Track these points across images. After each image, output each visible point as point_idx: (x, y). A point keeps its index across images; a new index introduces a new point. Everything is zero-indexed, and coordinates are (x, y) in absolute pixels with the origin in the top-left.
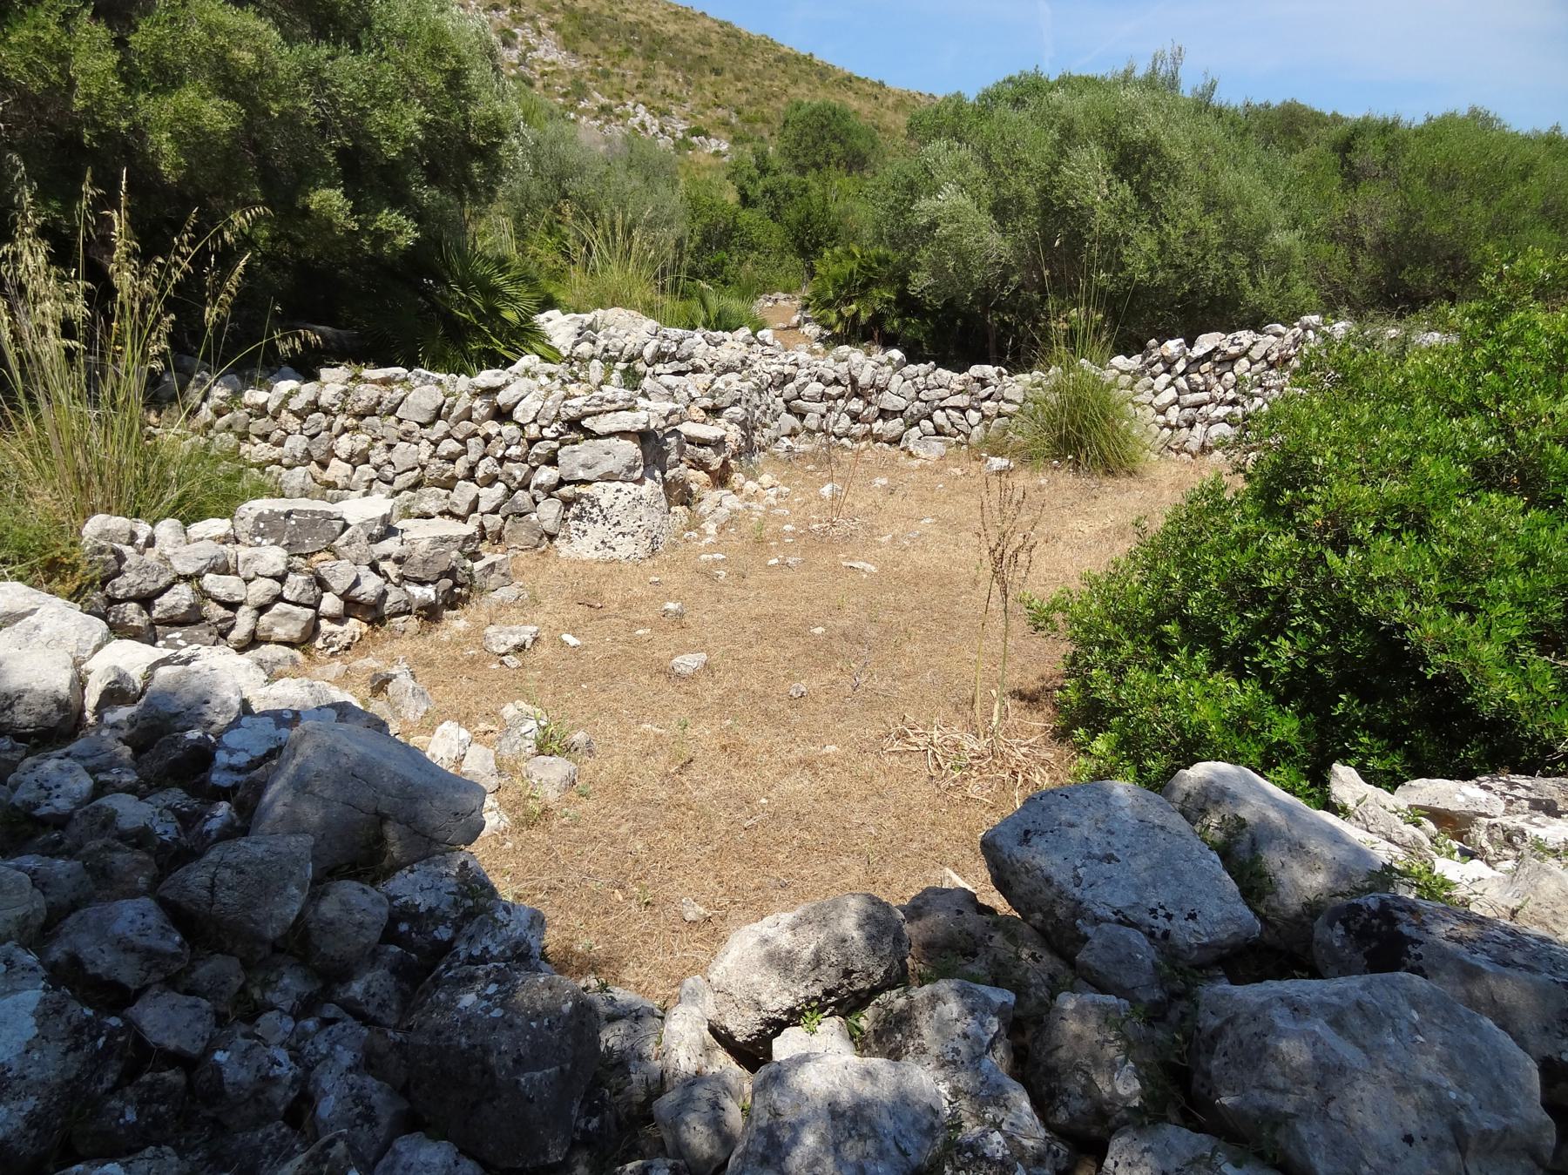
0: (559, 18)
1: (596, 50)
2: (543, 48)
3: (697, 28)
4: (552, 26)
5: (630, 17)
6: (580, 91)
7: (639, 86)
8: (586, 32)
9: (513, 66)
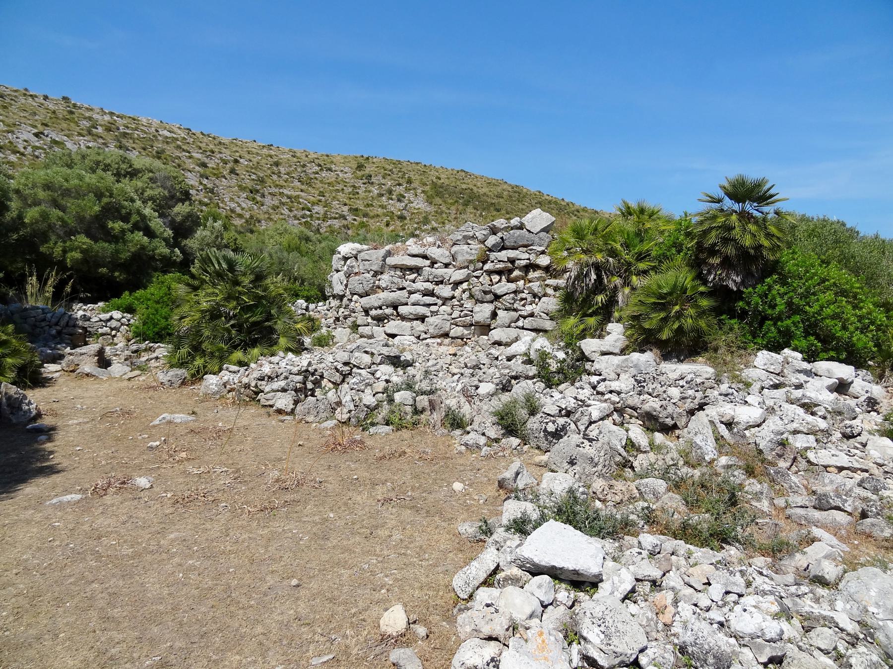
0: (427, 188)
1: (441, 202)
3: (499, 189)
4: (423, 192)
5: (464, 186)
6: (426, 221)
8: (438, 194)
9: (399, 210)
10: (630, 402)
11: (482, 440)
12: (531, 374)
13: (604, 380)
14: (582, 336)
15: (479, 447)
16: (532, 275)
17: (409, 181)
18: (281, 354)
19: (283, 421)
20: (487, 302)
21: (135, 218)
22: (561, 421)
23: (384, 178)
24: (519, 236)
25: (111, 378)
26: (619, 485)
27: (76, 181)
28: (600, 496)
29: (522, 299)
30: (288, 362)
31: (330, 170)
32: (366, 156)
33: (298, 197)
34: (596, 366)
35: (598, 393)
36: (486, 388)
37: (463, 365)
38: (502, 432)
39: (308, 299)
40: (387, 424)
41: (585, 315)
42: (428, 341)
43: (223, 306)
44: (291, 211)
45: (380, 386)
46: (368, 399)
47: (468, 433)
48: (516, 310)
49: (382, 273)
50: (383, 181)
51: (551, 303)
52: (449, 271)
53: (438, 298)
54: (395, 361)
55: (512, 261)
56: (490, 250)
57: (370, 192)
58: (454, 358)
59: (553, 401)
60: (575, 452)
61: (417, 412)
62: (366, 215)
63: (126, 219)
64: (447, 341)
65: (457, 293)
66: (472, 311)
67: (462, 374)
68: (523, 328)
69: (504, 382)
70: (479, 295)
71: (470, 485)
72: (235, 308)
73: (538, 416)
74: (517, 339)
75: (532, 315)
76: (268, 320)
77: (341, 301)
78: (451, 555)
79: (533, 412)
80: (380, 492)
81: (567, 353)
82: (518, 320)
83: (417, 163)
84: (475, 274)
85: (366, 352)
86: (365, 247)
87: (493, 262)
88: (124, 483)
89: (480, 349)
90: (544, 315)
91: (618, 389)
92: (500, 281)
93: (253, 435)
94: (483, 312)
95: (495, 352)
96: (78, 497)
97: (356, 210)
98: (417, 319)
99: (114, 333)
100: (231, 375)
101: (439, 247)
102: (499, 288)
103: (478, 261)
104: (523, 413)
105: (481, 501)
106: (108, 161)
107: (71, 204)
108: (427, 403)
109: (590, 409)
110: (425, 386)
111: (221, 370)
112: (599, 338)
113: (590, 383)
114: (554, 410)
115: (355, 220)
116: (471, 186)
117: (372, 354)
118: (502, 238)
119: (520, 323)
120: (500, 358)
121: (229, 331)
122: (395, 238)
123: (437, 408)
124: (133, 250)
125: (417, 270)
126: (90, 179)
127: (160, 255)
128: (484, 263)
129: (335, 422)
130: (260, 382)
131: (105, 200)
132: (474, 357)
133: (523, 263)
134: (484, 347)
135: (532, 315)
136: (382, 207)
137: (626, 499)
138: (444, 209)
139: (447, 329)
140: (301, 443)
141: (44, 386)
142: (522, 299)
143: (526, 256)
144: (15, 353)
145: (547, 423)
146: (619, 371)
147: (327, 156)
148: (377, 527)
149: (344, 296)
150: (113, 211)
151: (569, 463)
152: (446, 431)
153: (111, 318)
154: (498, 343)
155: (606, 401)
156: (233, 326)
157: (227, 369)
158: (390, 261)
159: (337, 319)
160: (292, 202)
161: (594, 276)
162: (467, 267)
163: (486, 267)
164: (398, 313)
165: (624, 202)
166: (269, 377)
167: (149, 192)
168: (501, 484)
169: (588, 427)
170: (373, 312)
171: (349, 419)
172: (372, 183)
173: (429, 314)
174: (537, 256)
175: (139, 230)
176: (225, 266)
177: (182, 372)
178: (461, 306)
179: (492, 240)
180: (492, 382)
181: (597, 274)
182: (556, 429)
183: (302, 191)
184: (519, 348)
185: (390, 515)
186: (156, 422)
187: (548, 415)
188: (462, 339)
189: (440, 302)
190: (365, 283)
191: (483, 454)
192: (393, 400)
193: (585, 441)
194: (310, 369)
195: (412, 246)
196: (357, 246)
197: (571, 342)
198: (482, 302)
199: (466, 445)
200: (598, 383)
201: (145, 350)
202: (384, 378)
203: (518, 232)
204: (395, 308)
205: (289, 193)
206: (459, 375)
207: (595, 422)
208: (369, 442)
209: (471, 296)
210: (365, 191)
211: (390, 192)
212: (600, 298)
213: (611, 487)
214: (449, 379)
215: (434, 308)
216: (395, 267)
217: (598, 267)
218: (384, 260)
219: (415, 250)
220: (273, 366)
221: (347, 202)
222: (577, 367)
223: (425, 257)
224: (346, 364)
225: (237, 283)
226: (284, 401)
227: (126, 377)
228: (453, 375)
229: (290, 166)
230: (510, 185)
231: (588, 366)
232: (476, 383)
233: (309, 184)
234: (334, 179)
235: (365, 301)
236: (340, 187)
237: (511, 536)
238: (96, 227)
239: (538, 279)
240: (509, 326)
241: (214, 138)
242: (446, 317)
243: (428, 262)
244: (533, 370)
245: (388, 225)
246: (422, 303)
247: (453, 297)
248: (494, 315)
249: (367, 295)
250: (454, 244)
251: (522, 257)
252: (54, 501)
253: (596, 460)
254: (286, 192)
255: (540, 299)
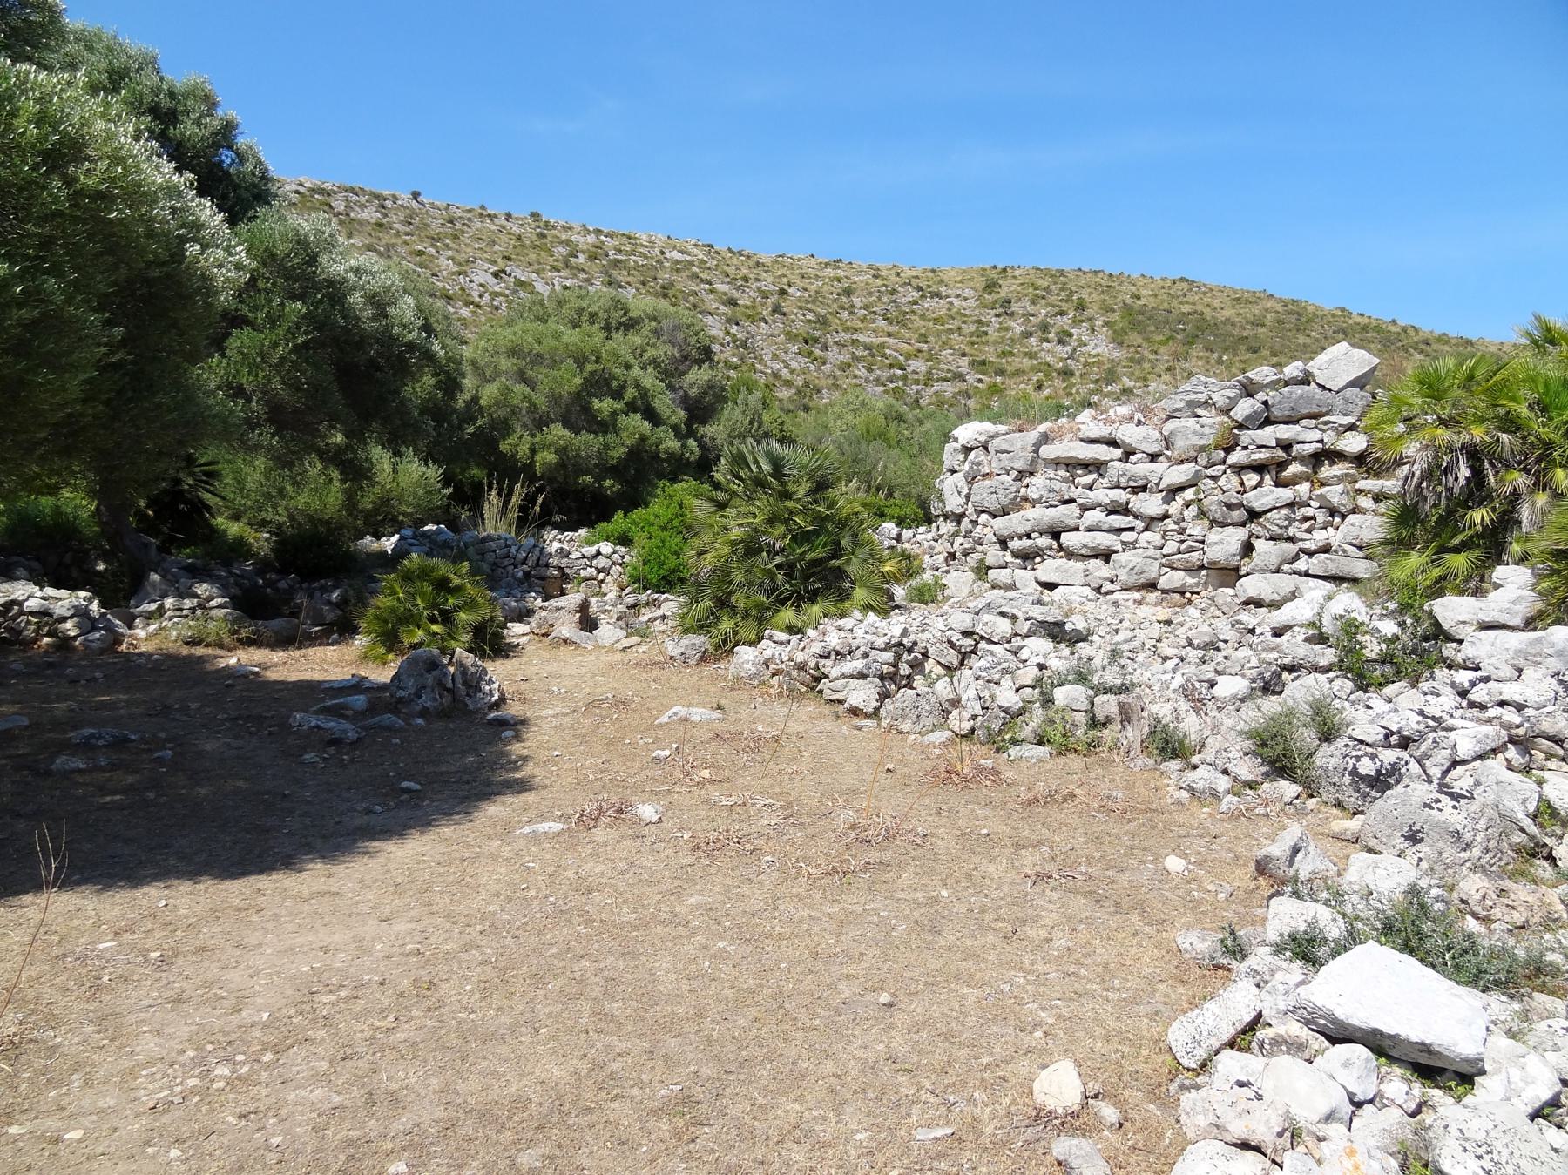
0: (1115, 317)
1: (1140, 341)
2: (1092, 344)
3: (1257, 310)
4: (1106, 324)
5: (1186, 309)
6: (1111, 376)
7: (1168, 369)
8: (1135, 326)
9: (1061, 359)
10: (1547, 726)
11: (1223, 783)
12: (1323, 662)
13: (1487, 679)
14: (1437, 589)
15: (1215, 795)
16: (1327, 471)
17: (1081, 307)
18: (857, 614)
19: (859, 728)
20: (1233, 525)
21: (631, 393)
22: (1389, 756)
23: (1033, 303)
24: (1301, 397)
25: (598, 647)
26: (1521, 892)
27: (553, 343)
28: (1478, 909)
29: (1306, 519)
30: (864, 629)
31: (938, 295)
32: (1000, 266)
33: (882, 346)
34: (1468, 651)
35: (1472, 705)
36: (1229, 686)
37: (1184, 642)
38: (1264, 769)
39: (901, 522)
40: (1041, 743)
41: (1443, 549)
42: (1117, 596)
43: (764, 533)
44: (870, 370)
45: (1028, 674)
46: (1007, 697)
47: (1195, 767)
48: (1291, 539)
49: (1031, 474)
50: (1031, 309)
51: (1370, 525)
52: (1159, 467)
53: (1136, 517)
54: (1056, 632)
55: (1286, 446)
56: (1241, 426)
57: (1007, 329)
58: (1166, 628)
59: (1369, 716)
60: (1421, 818)
61: (1094, 723)
62: (1000, 372)
63: (617, 395)
64: (1153, 596)
65: (1174, 507)
66: (1202, 542)
67: (1182, 659)
68: (1307, 574)
69: (1267, 675)
70: (1217, 511)
71: (1199, 864)
72: (783, 537)
73: (1340, 743)
74: (1293, 596)
75: (1326, 549)
76: (835, 556)
77: (959, 523)
78: (1163, 986)
79: (1328, 736)
80: (1030, 860)
81: (1402, 625)
82: (1296, 558)
83: (1096, 272)
84: (1210, 472)
85: (1003, 614)
86: (1002, 428)
87: (1246, 448)
88: (620, 811)
89: (1218, 613)
90: (1352, 550)
91: (1518, 699)
92: (1260, 484)
93: (812, 748)
94: (1224, 543)
95: (1248, 618)
96: (558, 826)
97: (984, 363)
98: (1096, 557)
99: (601, 576)
100: (776, 648)
101: (1139, 423)
102: (1258, 498)
103: (1216, 448)
104: (1308, 736)
105: (1221, 896)
106: (595, 308)
107: (542, 375)
108: (1115, 710)
109: (1452, 735)
110: (1111, 677)
111: (760, 638)
112: (1474, 594)
113: (1453, 685)
114: (1373, 734)
115: (980, 381)
116: (1199, 308)
117: (1014, 618)
118: (1265, 403)
119: (1301, 565)
120: (1258, 631)
121: (772, 577)
122: (1057, 411)
123: (1134, 718)
124: (628, 443)
125: (1097, 467)
126: (571, 337)
127: (666, 452)
128: (1229, 450)
129: (948, 734)
130: (823, 661)
131: (589, 367)
132: (1205, 628)
133: (1310, 449)
134: (1225, 609)
135: (1326, 549)
136: (1031, 355)
137: (1536, 919)
138: (1146, 353)
139: (1154, 575)
140: (891, 766)
141: (507, 656)
142: (1306, 519)
143: (1317, 435)
144: (471, 605)
145: (1358, 758)
146: (1521, 662)
147: (933, 271)
148: (1024, 922)
149: (963, 515)
150: (600, 384)
151: (1407, 838)
152: (1151, 762)
153: (599, 553)
154: (1257, 603)
155: (1489, 721)
156: (779, 567)
157: (771, 636)
158: (1048, 451)
159: (952, 556)
160: (873, 356)
161: (1464, 472)
162: (1195, 460)
163: (1233, 458)
164: (1060, 545)
165: (1538, 319)
166: (838, 653)
167: (651, 353)
168: (1262, 867)
169: (1448, 770)
170: (1015, 544)
171: (972, 731)
172: (1013, 314)
173: (1119, 547)
174: (1339, 434)
175: (635, 412)
176: (766, 467)
177: (700, 640)
178: (1182, 531)
179: (1244, 408)
180: (1243, 676)
181: (1471, 468)
182: (1379, 772)
183: (889, 335)
184: (1297, 613)
185: (1048, 902)
186: (664, 719)
187: (1362, 742)
188: (1183, 594)
189: (1140, 525)
190: (1001, 492)
191: (1223, 807)
192: (1052, 701)
193: (1442, 797)
194: (905, 641)
195: (1089, 424)
196: (988, 427)
197: (1410, 601)
198: (1224, 525)
199: (1190, 789)
200: (1473, 684)
201: (647, 604)
202: (1035, 660)
203: (1299, 390)
204: (1056, 536)
205: (868, 340)
206: (1176, 661)
207: (1464, 762)
208: (1008, 773)
209: (1202, 514)
210: (999, 330)
211: (1045, 328)
212: (1479, 516)
213: (1502, 893)
214: (1157, 666)
215: (1128, 536)
216: (1056, 463)
217: (1473, 454)
218: (1036, 451)
219: (1094, 429)
220: (843, 634)
221: (967, 350)
222: (1426, 649)
223: (1113, 443)
224: (967, 634)
225: (786, 495)
226: (862, 695)
227: (619, 646)
228: (1165, 659)
229: (870, 294)
230: (1281, 300)
231: (1448, 650)
232: (1211, 675)
233: (902, 323)
234: (944, 311)
235: (1000, 524)
236: (953, 325)
237: (1285, 965)
238: (578, 413)
239: (1340, 479)
240: (1278, 571)
241: (748, 257)
242: (1152, 552)
243: (1118, 453)
244: (1327, 656)
245: (1040, 387)
246: (1106, 527)
247: (1166, 516)
248: (1248, 549)
249: (1005, 514)
250: (1170, 417)
251: (1308, 437)
252: (527, 830)
253: (1468, 836)
254: (862, 338)
255: (1344, 517)
